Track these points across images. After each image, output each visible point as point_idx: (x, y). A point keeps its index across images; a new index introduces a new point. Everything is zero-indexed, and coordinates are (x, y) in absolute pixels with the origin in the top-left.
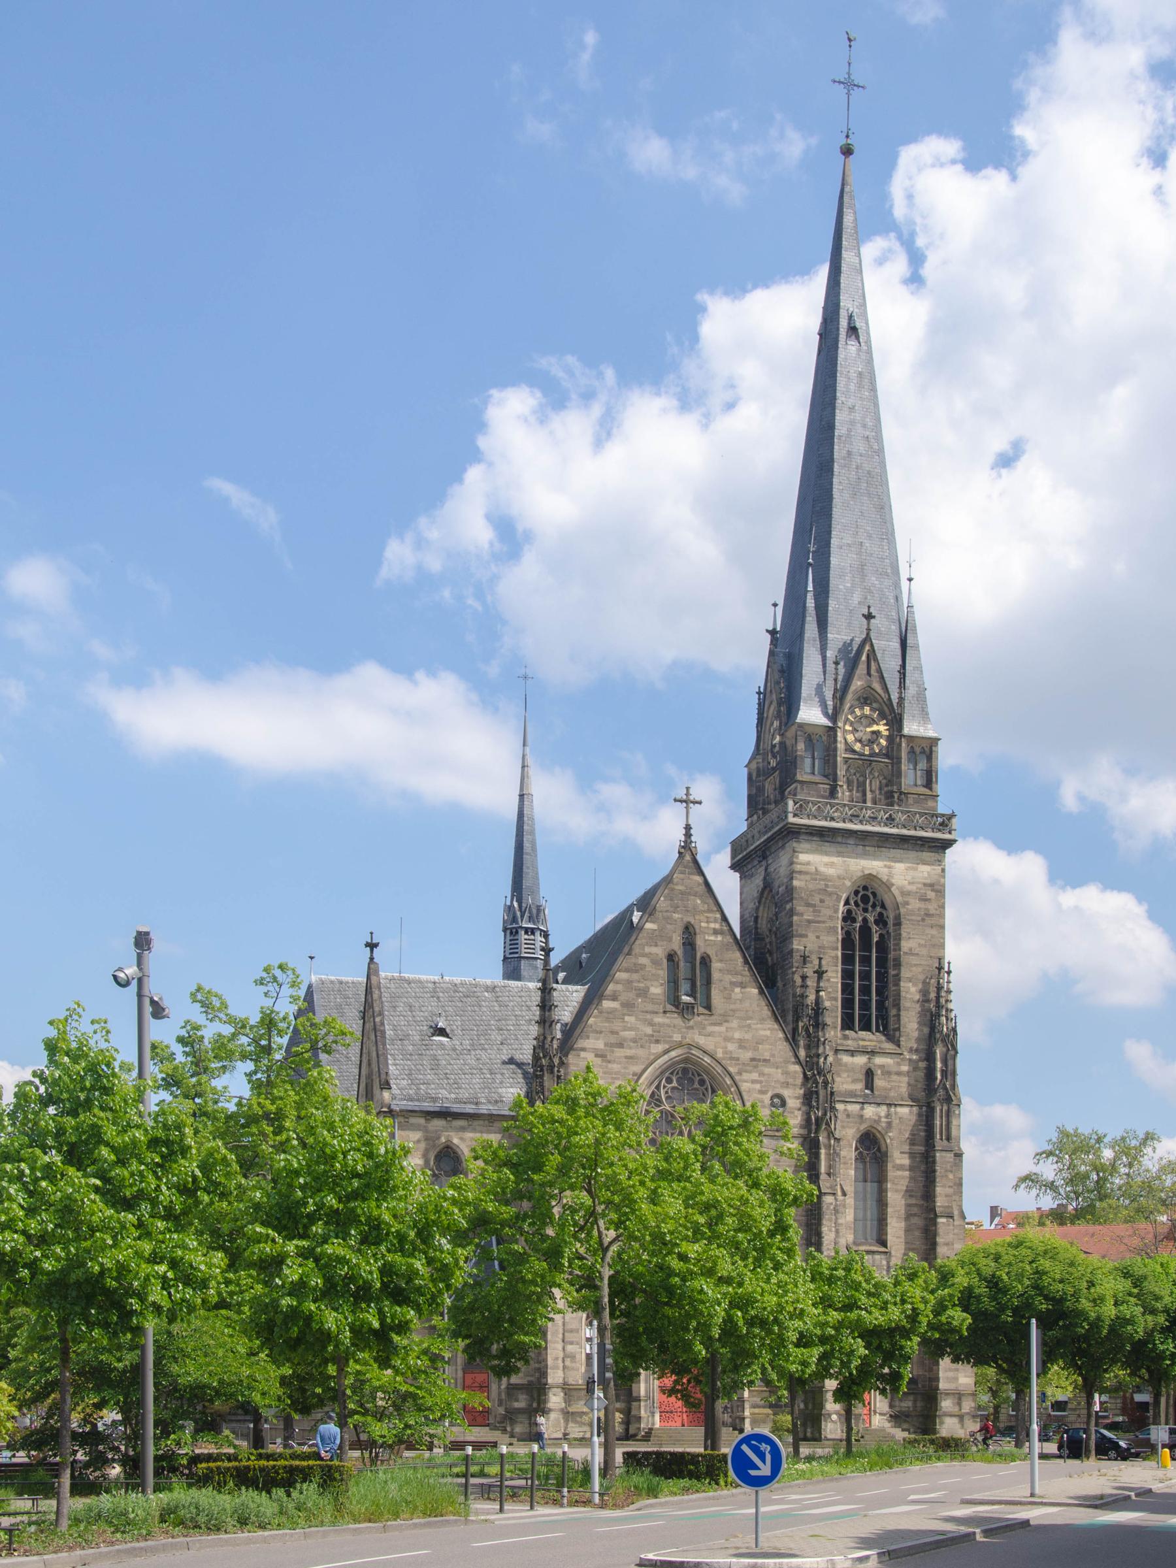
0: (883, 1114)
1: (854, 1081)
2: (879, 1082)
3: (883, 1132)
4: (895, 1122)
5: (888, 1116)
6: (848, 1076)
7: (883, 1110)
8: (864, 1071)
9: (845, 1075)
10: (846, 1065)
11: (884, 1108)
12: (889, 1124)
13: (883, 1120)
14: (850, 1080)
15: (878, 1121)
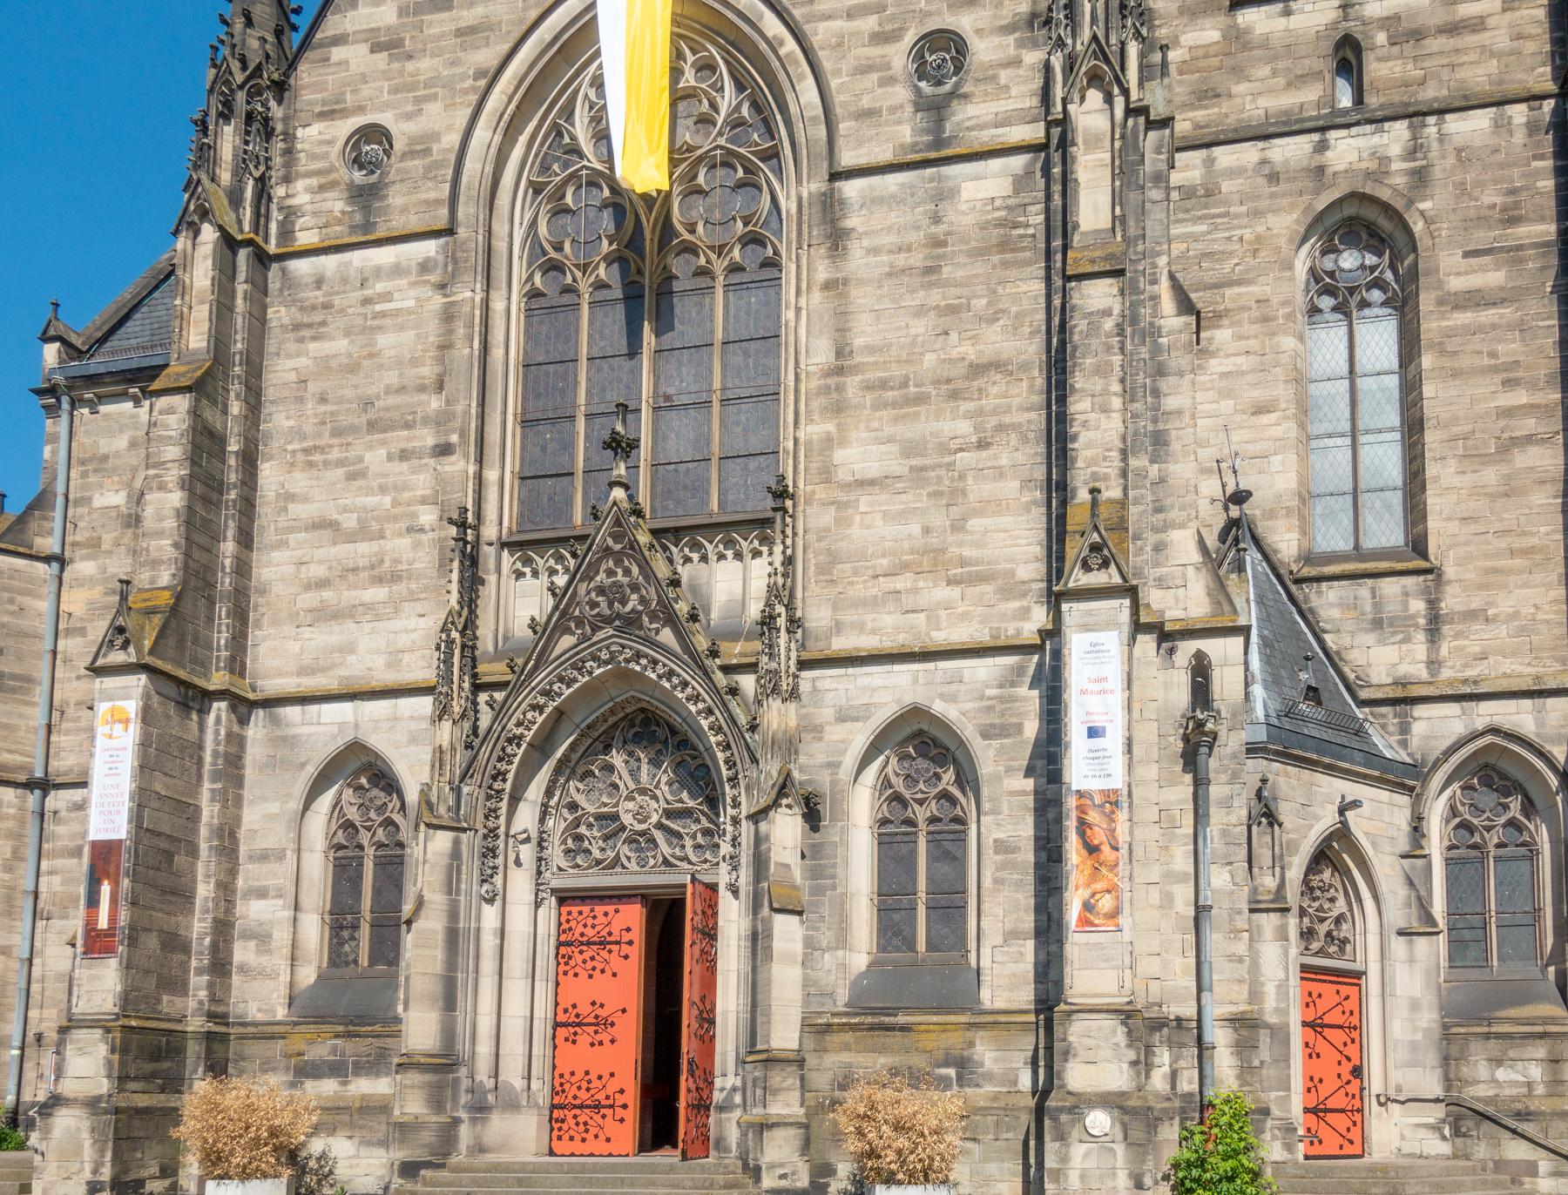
0: (1395, 150)
1: (1298, 81)
2: (1377, 69)
3: (1399, 204)
4: (1442, 165)
5: (1414, 149)
6: (1275, 73)
7: (1396, 135)
8: (1327, 47)
9: (1265, 71)
10: (1265, 43)
11: (1400, 129)
12: (1420, 178)
13: (1396, 166)
14: (1281, 81)
15: (1379, 173)
